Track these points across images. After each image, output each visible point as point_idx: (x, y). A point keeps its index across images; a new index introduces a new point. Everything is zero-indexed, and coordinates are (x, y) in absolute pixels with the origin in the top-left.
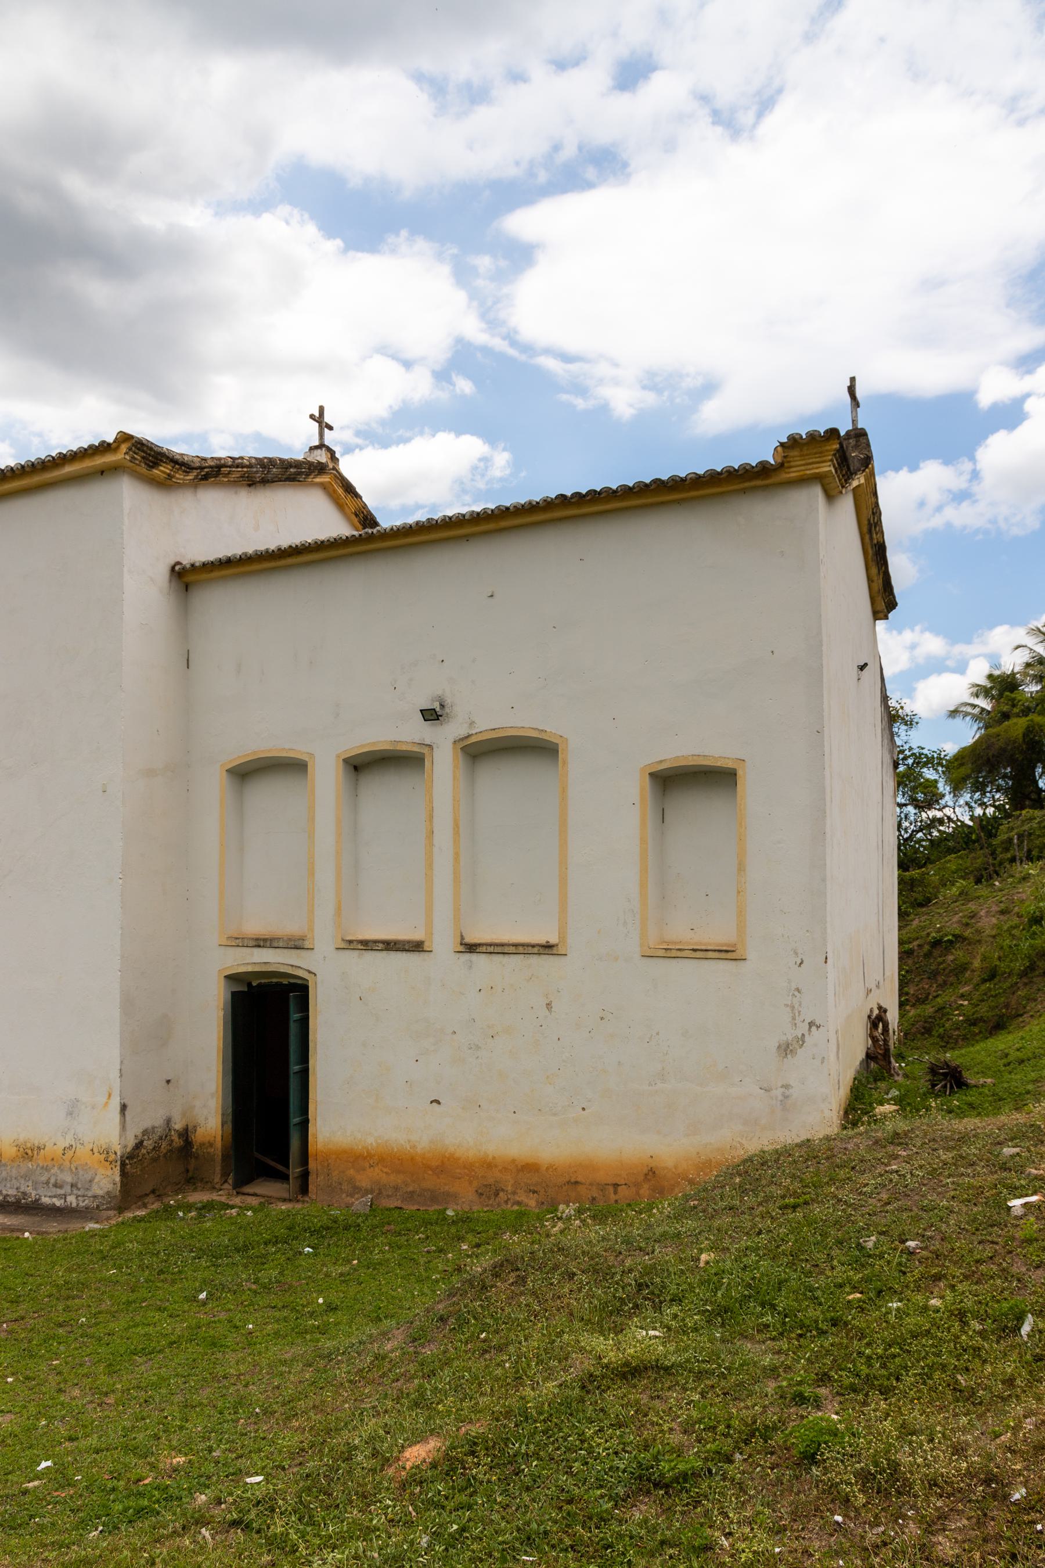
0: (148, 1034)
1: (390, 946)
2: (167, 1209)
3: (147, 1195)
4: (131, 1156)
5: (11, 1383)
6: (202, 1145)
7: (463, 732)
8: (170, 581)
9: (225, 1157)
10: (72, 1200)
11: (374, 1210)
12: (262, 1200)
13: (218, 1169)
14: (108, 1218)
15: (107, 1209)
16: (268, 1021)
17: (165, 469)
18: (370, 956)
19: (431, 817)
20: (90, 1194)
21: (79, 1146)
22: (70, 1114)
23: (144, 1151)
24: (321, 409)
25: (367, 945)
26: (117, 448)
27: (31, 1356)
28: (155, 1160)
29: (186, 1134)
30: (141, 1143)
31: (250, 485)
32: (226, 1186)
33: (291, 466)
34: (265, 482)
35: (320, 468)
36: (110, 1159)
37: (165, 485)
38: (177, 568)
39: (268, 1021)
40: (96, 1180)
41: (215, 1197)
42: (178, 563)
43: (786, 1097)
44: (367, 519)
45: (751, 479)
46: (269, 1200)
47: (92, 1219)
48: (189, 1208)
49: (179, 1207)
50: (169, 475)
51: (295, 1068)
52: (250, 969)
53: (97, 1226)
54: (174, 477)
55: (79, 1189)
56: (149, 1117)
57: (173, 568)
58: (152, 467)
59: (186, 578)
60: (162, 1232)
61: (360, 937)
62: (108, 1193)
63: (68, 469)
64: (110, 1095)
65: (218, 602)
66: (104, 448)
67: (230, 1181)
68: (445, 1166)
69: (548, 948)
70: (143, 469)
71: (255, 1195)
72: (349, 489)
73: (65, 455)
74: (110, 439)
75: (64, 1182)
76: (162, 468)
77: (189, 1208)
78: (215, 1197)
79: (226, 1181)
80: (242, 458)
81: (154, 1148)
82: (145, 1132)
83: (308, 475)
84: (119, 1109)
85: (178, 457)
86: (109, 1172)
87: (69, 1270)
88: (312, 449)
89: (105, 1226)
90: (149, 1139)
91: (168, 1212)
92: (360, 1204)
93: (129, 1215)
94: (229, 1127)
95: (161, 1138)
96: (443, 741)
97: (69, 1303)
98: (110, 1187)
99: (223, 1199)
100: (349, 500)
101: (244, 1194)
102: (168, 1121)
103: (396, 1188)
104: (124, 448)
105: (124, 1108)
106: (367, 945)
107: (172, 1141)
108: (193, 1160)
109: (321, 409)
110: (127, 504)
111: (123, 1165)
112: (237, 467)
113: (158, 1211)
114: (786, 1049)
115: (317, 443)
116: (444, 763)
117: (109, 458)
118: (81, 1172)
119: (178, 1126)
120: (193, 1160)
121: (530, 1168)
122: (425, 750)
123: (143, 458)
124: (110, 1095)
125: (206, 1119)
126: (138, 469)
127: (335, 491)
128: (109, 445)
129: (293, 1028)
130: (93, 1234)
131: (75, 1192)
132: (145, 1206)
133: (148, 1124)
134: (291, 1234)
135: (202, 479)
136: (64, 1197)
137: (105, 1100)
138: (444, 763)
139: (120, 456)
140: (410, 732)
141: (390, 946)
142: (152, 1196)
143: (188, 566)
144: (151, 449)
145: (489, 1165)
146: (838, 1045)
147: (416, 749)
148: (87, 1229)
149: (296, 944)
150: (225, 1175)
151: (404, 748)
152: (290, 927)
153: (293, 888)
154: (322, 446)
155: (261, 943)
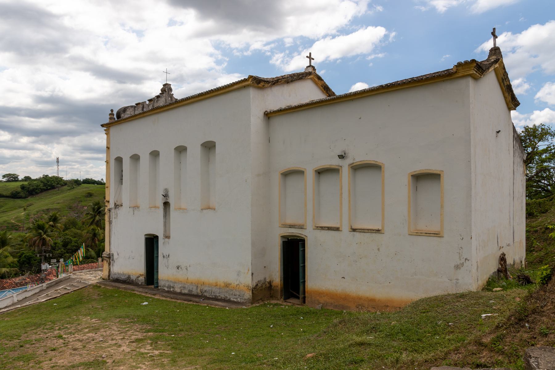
0: (259, 253)
1: (329, 229)
2: (265, 304)
4: (254, 288)
7: (351, 162)
9: (281, 291)
10: (239, 299)
13: (279, 294)
16: (293, 251)
18: (323, 232)
19: (342, 189)
22: (238, 275)
25: (322, 228)
28: (261, 290)
29: (270, 283)
34: (292, 81)
39: (293, 251)
41: (278, 302)
43: (457, 283)
44: (326, 89)
45: (445, 77)
46: (294, 304)
48: (271, 304)
49: (268, 304)
51: (301, 265)
52: (288, 234)
56: (260, 277)
60: (262, 310)
61: (321, 226)
68: (346, 298)
69: (378, 231)
77: (271, 304)
78: (278, 302)
82: (258, 282)
87: (238, 317)
89: (248, 307)
93: (254, 305)
94: (282, 281)
96: (345, 165)
98: (249, 297)
102: (265, 279)
103: (332, 304)
105: (252, 274)
106: (322, 228)
111: (252, 291)
114: (457, 267)
116: (346, 172)
119: (268, 280)
121: (373, 300)
122: (340, 168)
129: (301, 253)
130: (244, 309)
132: (259, 303)
133: (259, 279)
138: (346, 172)
140: (335, 162)
141: (329, 229)
145: (360, 298)
146: (478, 267)
147: (337, 167)
149: (301, 227)
150: (281, 296)
151: (333, 167)
152: (300, 222)
153: (301, 210)
155: (291, 226)
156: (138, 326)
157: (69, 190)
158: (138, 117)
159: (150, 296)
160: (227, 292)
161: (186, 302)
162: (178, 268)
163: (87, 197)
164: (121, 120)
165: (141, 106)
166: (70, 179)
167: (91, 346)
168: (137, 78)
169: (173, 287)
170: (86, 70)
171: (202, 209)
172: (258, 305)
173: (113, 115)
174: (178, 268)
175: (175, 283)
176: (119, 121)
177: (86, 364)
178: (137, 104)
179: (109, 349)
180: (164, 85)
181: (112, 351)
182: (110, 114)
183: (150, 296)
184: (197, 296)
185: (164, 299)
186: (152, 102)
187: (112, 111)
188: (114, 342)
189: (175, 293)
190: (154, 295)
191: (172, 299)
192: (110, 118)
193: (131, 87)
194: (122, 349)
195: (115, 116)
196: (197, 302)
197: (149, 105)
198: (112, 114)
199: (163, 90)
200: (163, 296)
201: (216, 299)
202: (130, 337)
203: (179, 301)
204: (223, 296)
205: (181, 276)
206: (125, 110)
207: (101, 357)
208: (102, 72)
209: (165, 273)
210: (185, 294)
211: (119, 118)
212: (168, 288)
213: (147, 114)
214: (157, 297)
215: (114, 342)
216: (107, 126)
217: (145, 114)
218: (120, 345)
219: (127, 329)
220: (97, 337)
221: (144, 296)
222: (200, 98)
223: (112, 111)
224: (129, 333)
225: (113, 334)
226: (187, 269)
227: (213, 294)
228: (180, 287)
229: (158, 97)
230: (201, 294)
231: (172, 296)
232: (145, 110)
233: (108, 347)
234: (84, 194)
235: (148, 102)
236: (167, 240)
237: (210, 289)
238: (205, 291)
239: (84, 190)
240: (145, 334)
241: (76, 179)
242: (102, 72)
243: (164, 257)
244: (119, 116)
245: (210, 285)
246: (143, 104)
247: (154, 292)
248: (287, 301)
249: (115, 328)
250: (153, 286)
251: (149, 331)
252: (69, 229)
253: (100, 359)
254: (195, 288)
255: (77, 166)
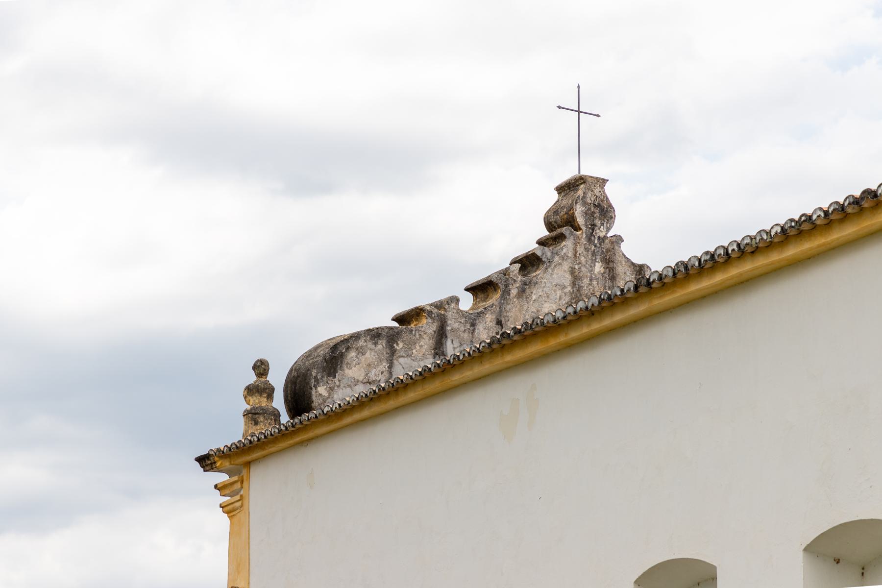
158: (411, 395)
164: (316, 422)
165: (428, 327)
168: (390, 159)
173: (268, 391)
176: (305, 428)
178: (403, 319)
180: (566, 188)
182: (251, 390)
186: (495, 298)
187: (261, 368)
192: (252, 416)
193: (365, 213)
195: (279, 402)
197: (472, 320)
198: (259, 389)
199: (559, 225)
206: (333, 357)
213: (469, 373)
216: (234, 464)
217: (456, 377)
223: (261, 368)
229: (528, 263)
232: (451, 349)
235: (467, 302)
244: (299, 398)
246: (439, 312)
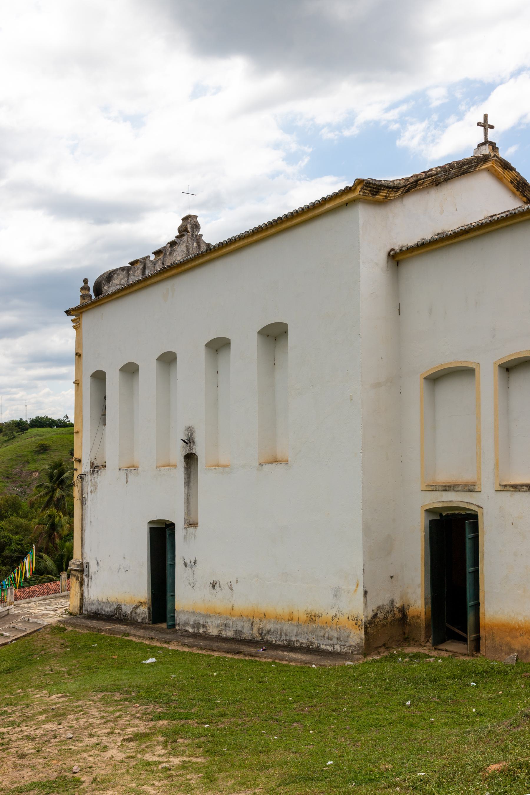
0: (379, 548)
2: (392, 656)
3: (380, 647)
4: (371, 622)
5: (312, 734)
6: (413, 617)
8: (388, 262)
9: (427, 626)
10: (337, 647)
11: (519, 663)
12: (451, 654)
13: (423, 633)
14: (358, 660)
15: (358, 654)
17: (383, 193)
20: (347, 644)
21: (341, 615)
23: (378, 620)
24: (486, 117)
26: (355, 189)
27: (320, 723)
28: (384, 625)
29: (403, 610)
30: (376, 614)
31: (437, 185)
32: (428, 644)
33: (464, 165)
35: (485, 159)
36: (359, 624)
37: (384, 202)
38: (391, 253)
40: (351, 636)
42: (392, 250)
46: (454, 654)
47: (349, 659)
50: (386, 196)
53: (351, 663)
54: (389, 196)
55: (341, 641)
56: (381, 599)
57: (389, 254)
58: (376, 195)
59: (397, 258)
62: (358, 644)
63: (328, 206)
64: (357, 585)
65: (417, 270)
66: (348, 190)
67: (431, 641)
70: (370, 197)
71: (446, 651)
72: (506, 166)
73: (326, 199)
74: (351, 185)
75: (333, 636)
76: (381, 194)
79: (428, 641)
80: (431, 170)
81: (384, 618)
82: (378, 608)
83: (476, 166)
84: (363, 593)
85: (391, 184)
86: (358, 632)
87: (337, 685)
88: (479, 146)
89: (357, 663)
90: (381, 613)
91: (393, 658)
92: (510, 659)
93: (370, 658)
95: (388, 612)
97: (338, 700)
98: (359, 641)
99: (426, 652)
100: (508, 176)
101: (439, 650)
102: (392, 602)
104: (359, 188)
105: (366, 593)
107: (395, 614)
108: (408, 627)
109: (486, 117)
110: (361, 222)
111: (366, 628)
112: (428, 177)
113: (386, 657)
115: (483, 141)
117: (351, 196)
118: (342, 631)
119: (398, 605)
120: (408, 627)
123: (370, 191)
124: (357, 585)
125: (415, 601)
126: (367, 198)
127: (496, 170)
128: (350, 188)
130: (349, 667)
131: (339, 643)
132: (379, 653)
133: (380, 603)
134: (465, 673)
135: (406, 192)
136: (333, 645)
137: (355, 588)
139: (356, 194)
142: (383, 648)
143: (398, 251)
144: (375, 184)
148: (346, 665)
150: (427, 637)
154: (486, 142)
156: (138, 708)
157: (6, 441)
158: (135, 288)
159: (158, 644)
160: (312, 633)
161: (230, 656)
162: (213, 587)
163: (39, 452)
164: (104, 298)
165: (140, 266)
166: (7, 421)
167: (52, 749)
168: (129, 211)
169: (204, 626)
170: (37, 205)
171: (261, 464)
172: (377, 657)
173: (88, 289)
174: (213, 587)
175: (208, 616)
176: (100, 300)
177: (44, 786)
178: (132, 264)
179: (85, 755)
180: (185, 219)
181: (91, 759)
182: (82, 289)
183: (158, 644)
184: (251, 642)
185: (186, 650)
186: (161, 256)
187: (86, 281)
188: (94, 740)
189: (207, 637)
190: (168, 642)
191: (202, 649)
192: (83, 297)
193: (120, 229)
194: (109, 754)
195: (92, 292)
196: (251, 655)
197: (154, 263)
198: (86, 288)
199: (183, 231)
200: (184, 644)
201: (290, 647)
202: (123, 730)
203: (216, 654)
204: (304, 641)
205: (219, 602)
206: (109, 277)
207: (71, 770)
208: (67, 207)
209: (189, 598)
210: (227, 640)
211: (99, 294)
212: (193, 627)
213: (153, 281)
214: (172, 647)
215: (94, 740)
216: (76, 313)
217: (149, 282)
218: (106, 747)
219: (117, 714)
220: (62, 731)
221: (148, 646)
222: (255, 238)
223: (86, 281)
224: (122, 721)
225: (91, 724)
226: (231, 588)
227: (284, 637)
228: (218, 626)
229: (172, 244)
230: (259, 639)
231: (202, 643)
232: (148, 273)
233: (83, 751)
234: (33, 449)
235: (153, 257)
236: (191, 530)
237: (278, 626)
238: (269, 632)
239: (33, 439)
240: (152, 724)
241: (18, 419)
242: (67, 207)
243: (185, 565)
244: (98, 290)
245: (278, 619)
246: (144, 261)
247: (168, 637)
248: (441, 647)
249: (94, 711)
250: (164, 626)
251: (159, 717)
252: (6, 517)
253: (69, 775)
254: (247, 626)
255: (20, 394)
